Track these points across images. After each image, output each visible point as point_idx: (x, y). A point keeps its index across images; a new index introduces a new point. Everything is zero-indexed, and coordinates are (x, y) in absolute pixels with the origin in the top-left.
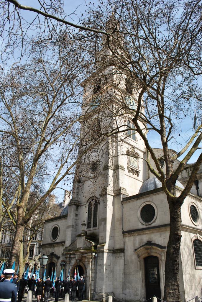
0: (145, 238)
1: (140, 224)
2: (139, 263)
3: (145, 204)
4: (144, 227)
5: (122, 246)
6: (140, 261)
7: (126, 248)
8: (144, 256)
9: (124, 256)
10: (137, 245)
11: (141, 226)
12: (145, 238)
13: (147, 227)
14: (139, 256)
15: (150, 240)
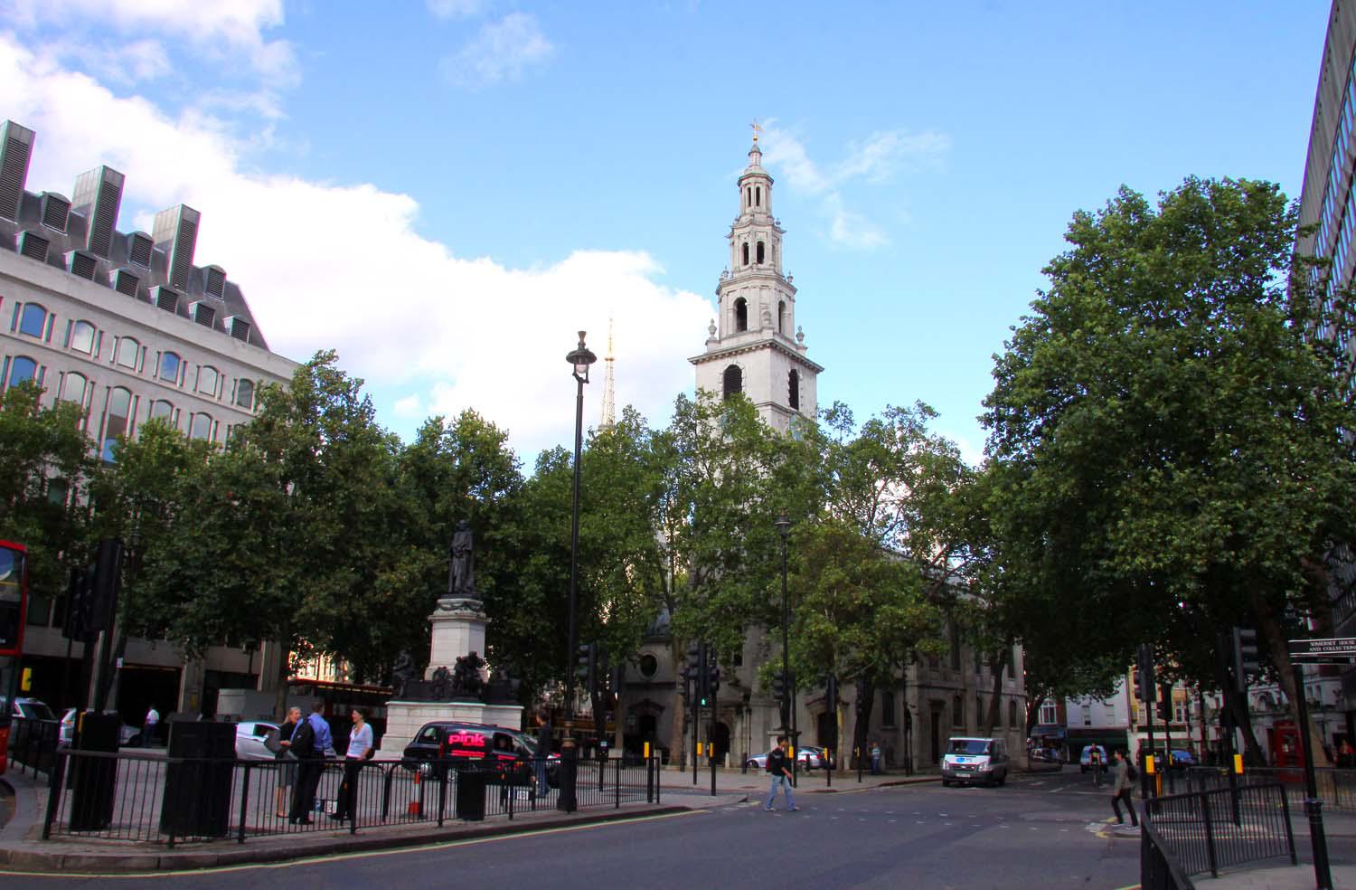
8: (819, 712)
14: (812, 713)
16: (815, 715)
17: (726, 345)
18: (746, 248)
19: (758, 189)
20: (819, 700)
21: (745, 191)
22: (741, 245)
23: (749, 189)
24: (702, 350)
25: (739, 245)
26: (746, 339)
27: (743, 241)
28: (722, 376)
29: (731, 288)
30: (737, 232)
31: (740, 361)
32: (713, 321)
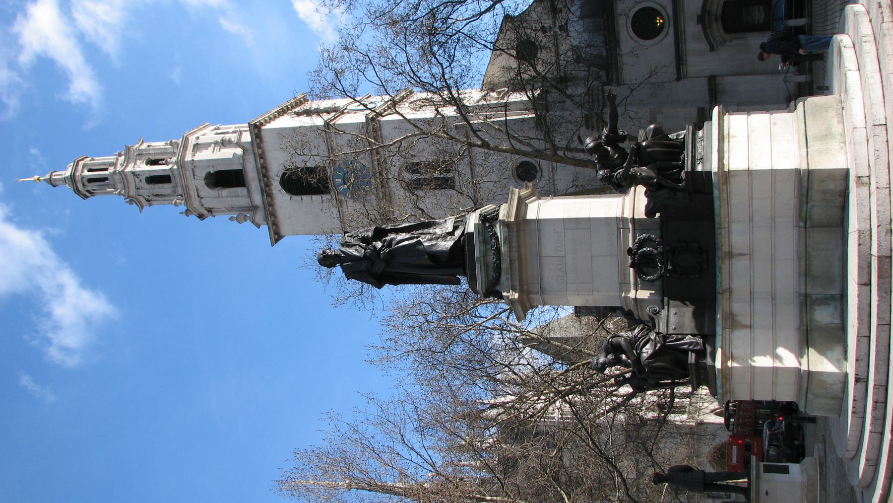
0: (692, 28)
1: (667, 41)
2: (734, 42)
3: (630, 29)
4: (671, 30)
5: (704, 82)
6: (731, 40)
7: (708, 74)
8: (722, 31)
9: (722, 76)
10: (705, 46)
11: (670, 40)
12: (692, 28)
13: (672, 23)
14: (724, 42)
15: (695, 19)
16: (727, 37)
17: (258, 199)
18: (154, 180)
19: (90, 170)
20: (705, 29)
21: (91, 187)
22: (148, 186)
23: (91, 180)
24: (265, 228)
25: (149, 190)
26: (252, 174)
27: (144, 184)
28: (294, 197)
29: (193, 193)
30: (132, 192)
31: (276, 170)
32: (231, 219)
